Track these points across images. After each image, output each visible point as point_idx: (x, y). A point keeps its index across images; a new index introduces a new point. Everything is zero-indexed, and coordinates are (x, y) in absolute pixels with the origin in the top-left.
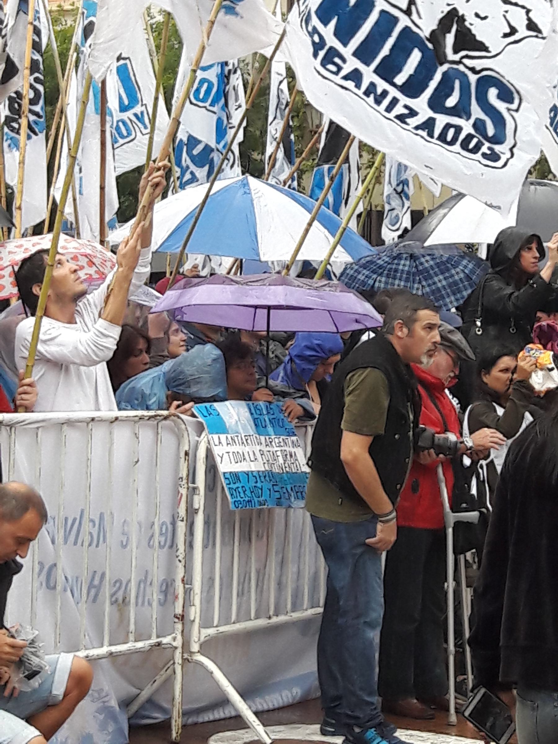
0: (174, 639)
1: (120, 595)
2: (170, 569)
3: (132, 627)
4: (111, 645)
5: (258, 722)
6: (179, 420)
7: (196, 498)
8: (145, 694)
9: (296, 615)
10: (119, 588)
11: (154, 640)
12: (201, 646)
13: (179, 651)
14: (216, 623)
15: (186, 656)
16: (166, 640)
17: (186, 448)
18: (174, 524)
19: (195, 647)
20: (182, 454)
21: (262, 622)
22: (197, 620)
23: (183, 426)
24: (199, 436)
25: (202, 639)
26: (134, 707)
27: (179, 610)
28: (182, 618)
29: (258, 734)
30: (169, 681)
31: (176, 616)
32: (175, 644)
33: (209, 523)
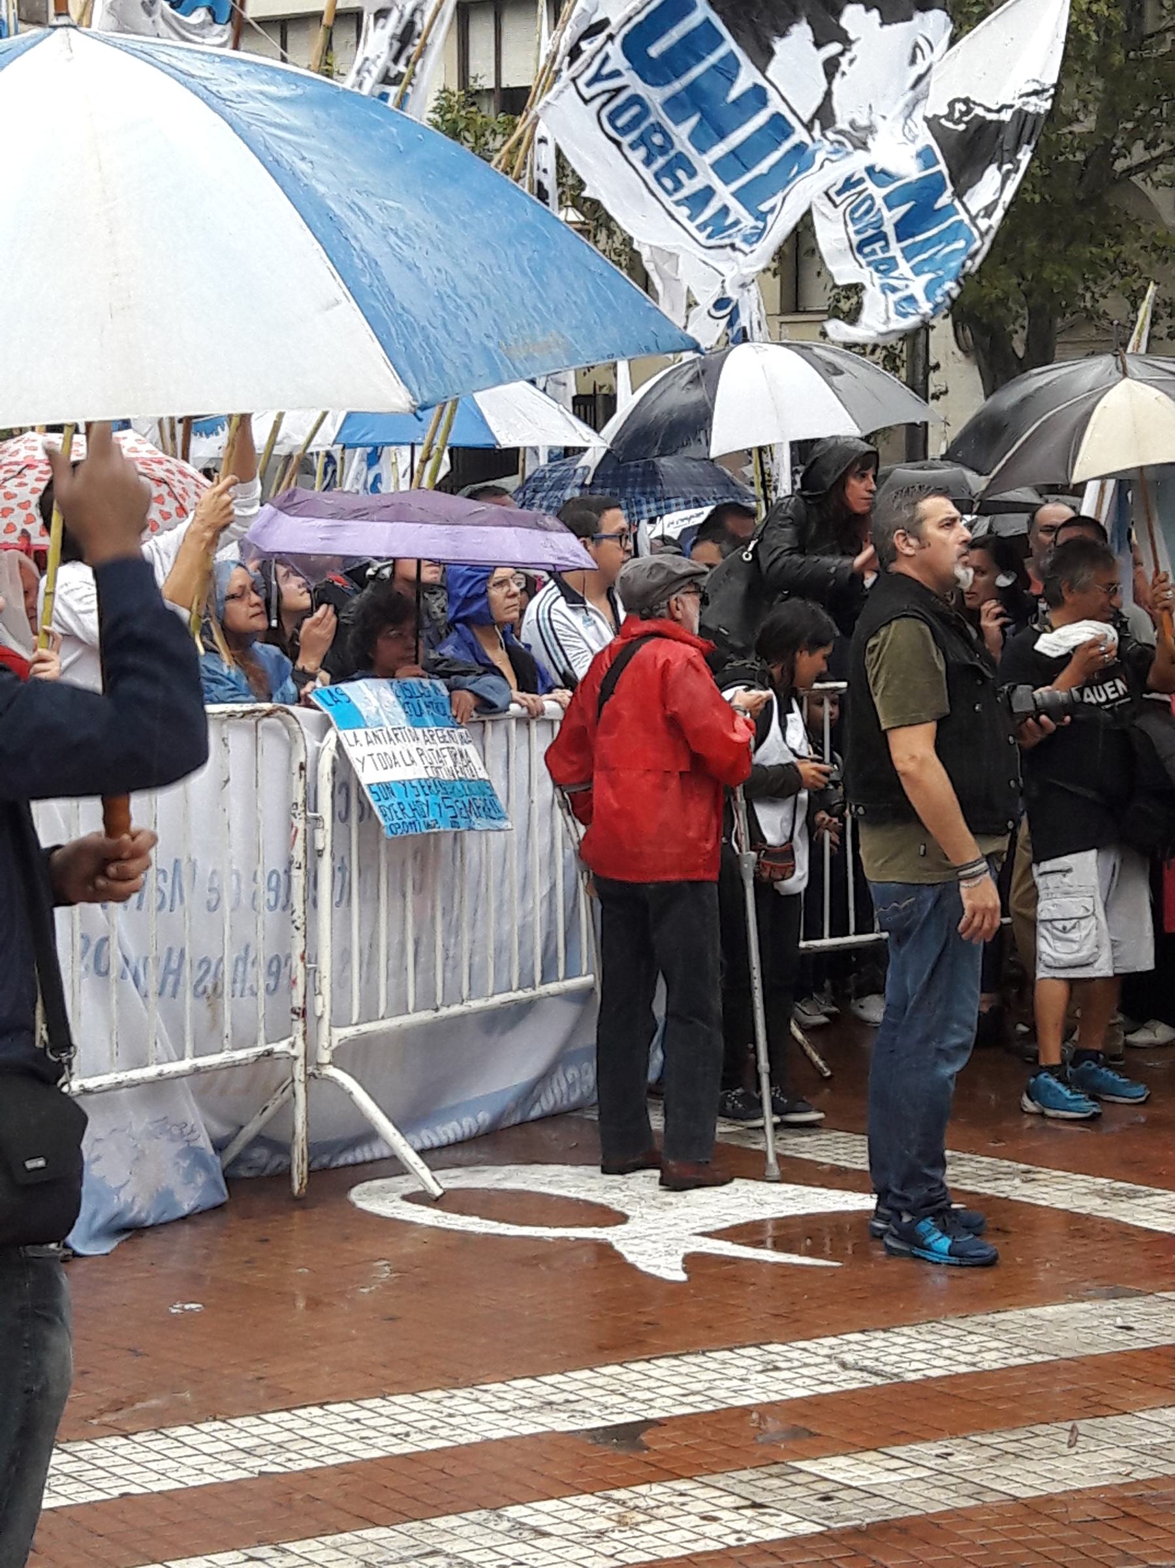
0: (293, 1045)
1: (208, 982)
2: (284, 940)
3: (227, 1030)
4: (195, 1056)
5: (421, 1164)
6: (290, 717)
7: (319, 834)
8: (251, 1130)
9: (476, 1004)
10: (207, 971)
11: (261, 1049)
12: (334, 1053)
13: (301, 1061)
14: (355, 1019)
15: (310, 1069)
16: (281, 1046)
17: (302, 759)
18: (288, 872)
19: (325, 1057)
20: (296, 768)
21: (426, 1016)
22: (327, 1016)
23: (297, 726)
24: (321, 741)
25: (335, 1044)
26: (235, 1149)
27: (298, 1002)
28: (302, 1013)
29: (423, 1182)
30: (287, 1110)
31: (294, 1011)
32: (293, 1052)
33: (341, 868)
